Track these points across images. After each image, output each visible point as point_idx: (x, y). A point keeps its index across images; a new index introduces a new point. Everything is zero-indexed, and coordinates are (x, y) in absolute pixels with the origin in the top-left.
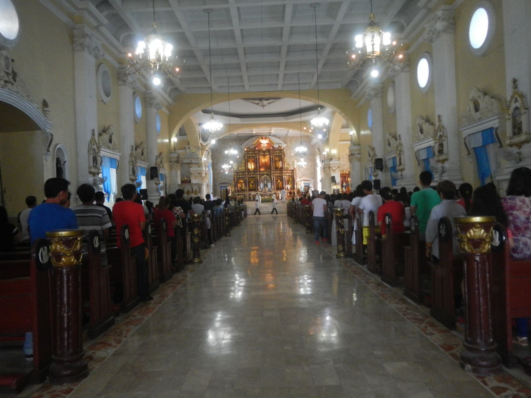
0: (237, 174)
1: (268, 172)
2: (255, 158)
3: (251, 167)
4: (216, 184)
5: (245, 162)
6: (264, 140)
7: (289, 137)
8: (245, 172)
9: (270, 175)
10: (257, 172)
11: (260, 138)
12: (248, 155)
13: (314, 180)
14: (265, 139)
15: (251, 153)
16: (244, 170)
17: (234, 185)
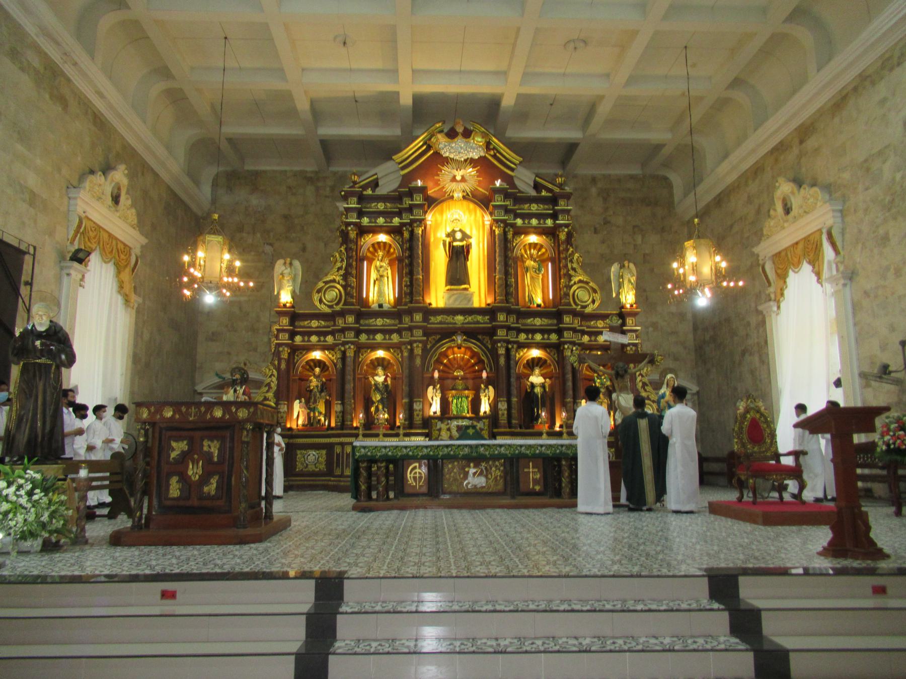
0: (292, 323)
1: (479, 318)
2: (406, 235)
3: (381, 293)
4: (199, 388)
5: (348, 258)
6: (460, 137)
7: (575, 176)
8: (342, 314)
9: (487, 339)
10: (410, 312)
11: (441, 132)
12: (365, 221)
13: (699, 383)
14: (467, 134)
15: (381, 206)
16: (338, 308)
17: (274, 385)
